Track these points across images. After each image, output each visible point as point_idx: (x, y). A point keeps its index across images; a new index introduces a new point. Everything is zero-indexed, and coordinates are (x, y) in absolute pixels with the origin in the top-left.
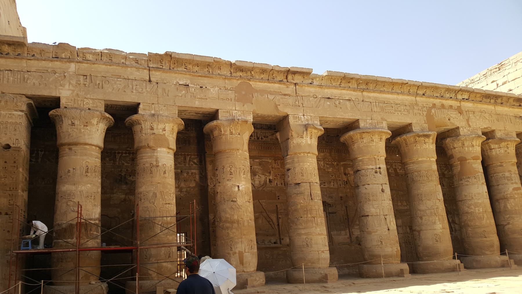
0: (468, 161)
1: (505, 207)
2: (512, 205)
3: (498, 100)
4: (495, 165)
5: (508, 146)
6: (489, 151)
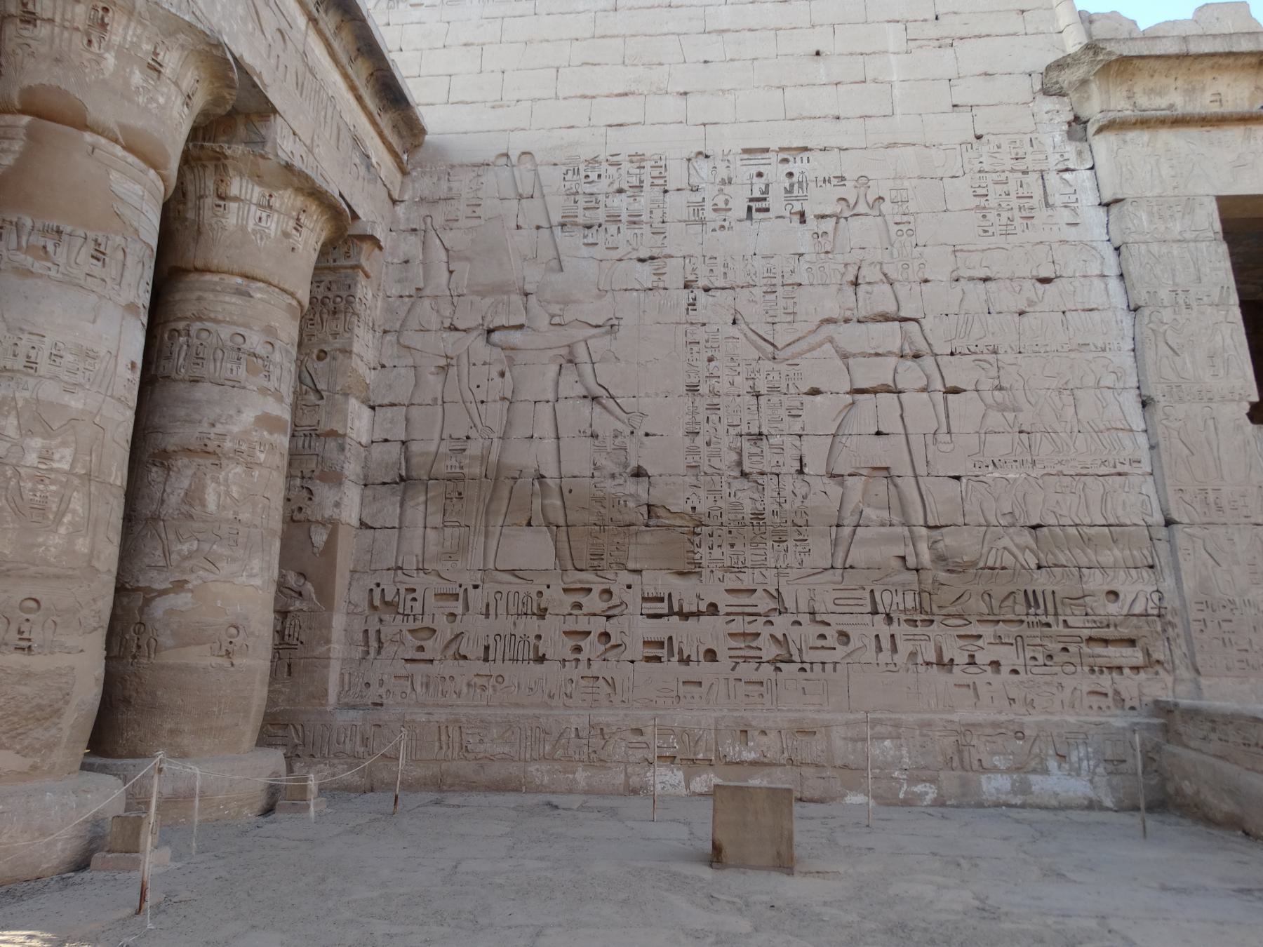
0: (88, 137)
1: (193, 496)
2: (228, 493)
3: (326, 12)
4: (216, 278)
5: (303, 217)
6: (210, 201)
